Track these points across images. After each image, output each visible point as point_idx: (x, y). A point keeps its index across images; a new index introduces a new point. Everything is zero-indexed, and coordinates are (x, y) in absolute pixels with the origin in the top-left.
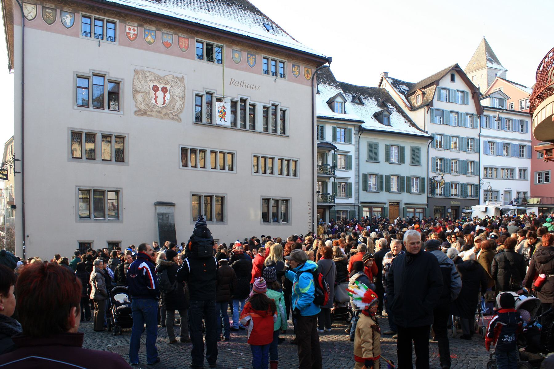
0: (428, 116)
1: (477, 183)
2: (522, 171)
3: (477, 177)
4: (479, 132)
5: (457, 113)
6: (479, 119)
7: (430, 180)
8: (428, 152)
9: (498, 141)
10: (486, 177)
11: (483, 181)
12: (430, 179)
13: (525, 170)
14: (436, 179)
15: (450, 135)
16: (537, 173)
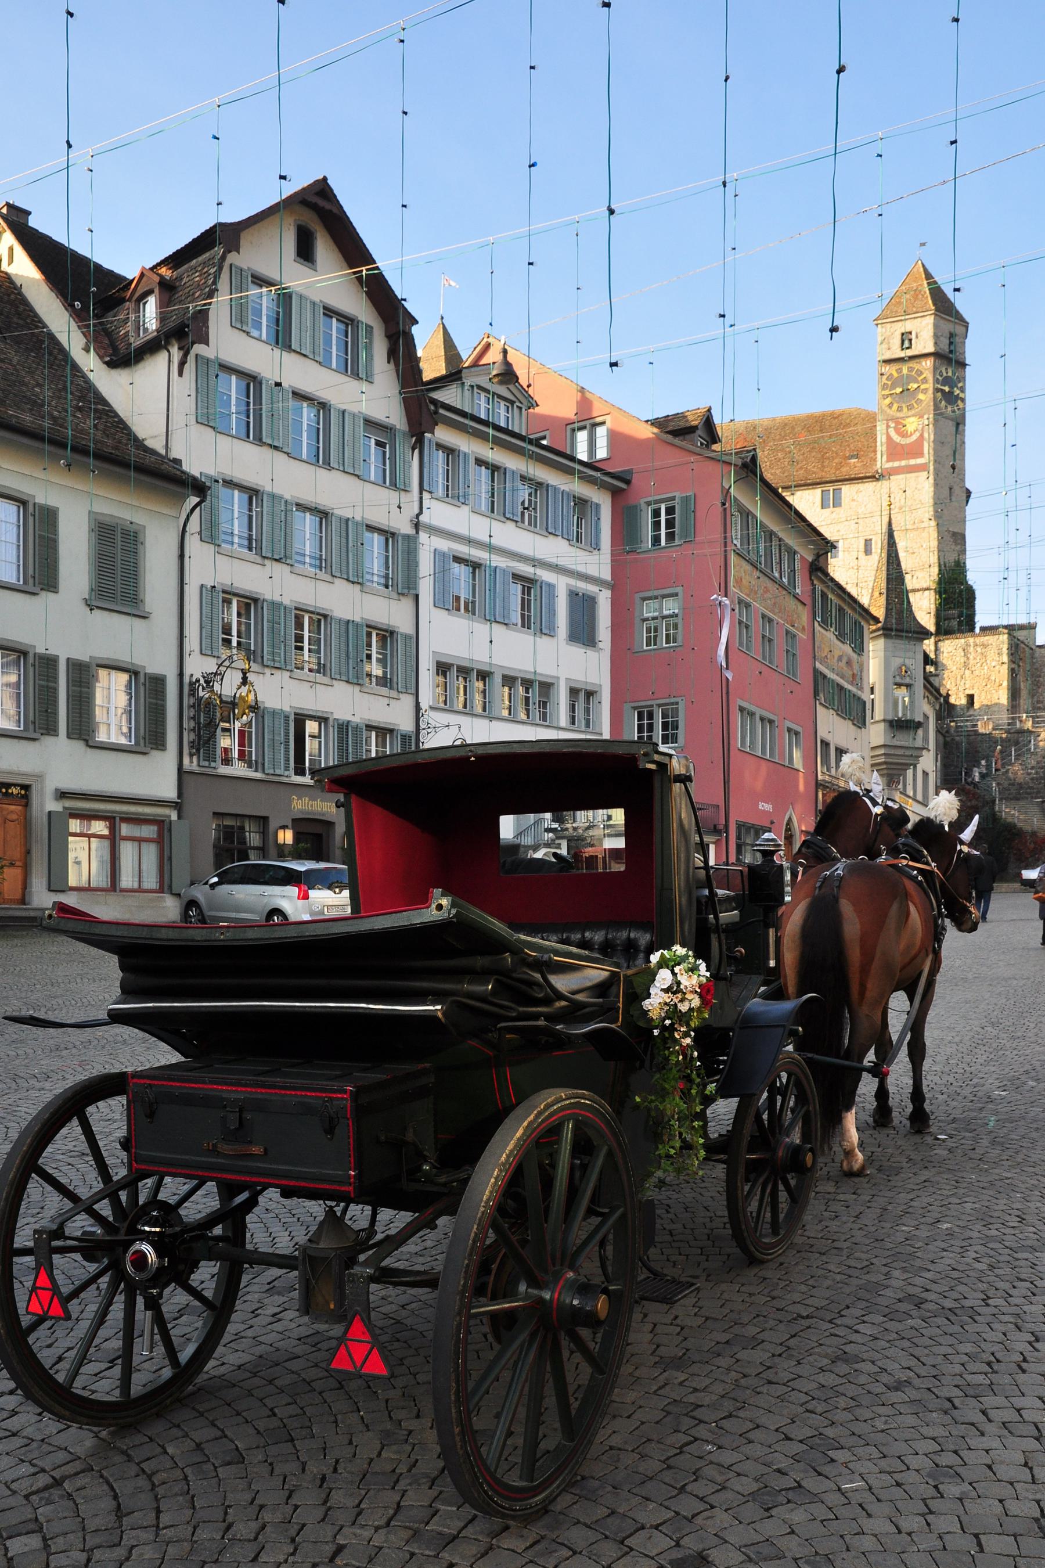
0: (185, 386)
1: (406, 725)
3: (407, 702)
4: (416, 511)
5: (323, 406)
6: (416, 451)
7: (193, 691)
8: (182, 556)
10: (446, 706)
12: (191, 684)
13: (589, 694)
14: (217, 687)
15: (287, 496)
16: (635, 708)
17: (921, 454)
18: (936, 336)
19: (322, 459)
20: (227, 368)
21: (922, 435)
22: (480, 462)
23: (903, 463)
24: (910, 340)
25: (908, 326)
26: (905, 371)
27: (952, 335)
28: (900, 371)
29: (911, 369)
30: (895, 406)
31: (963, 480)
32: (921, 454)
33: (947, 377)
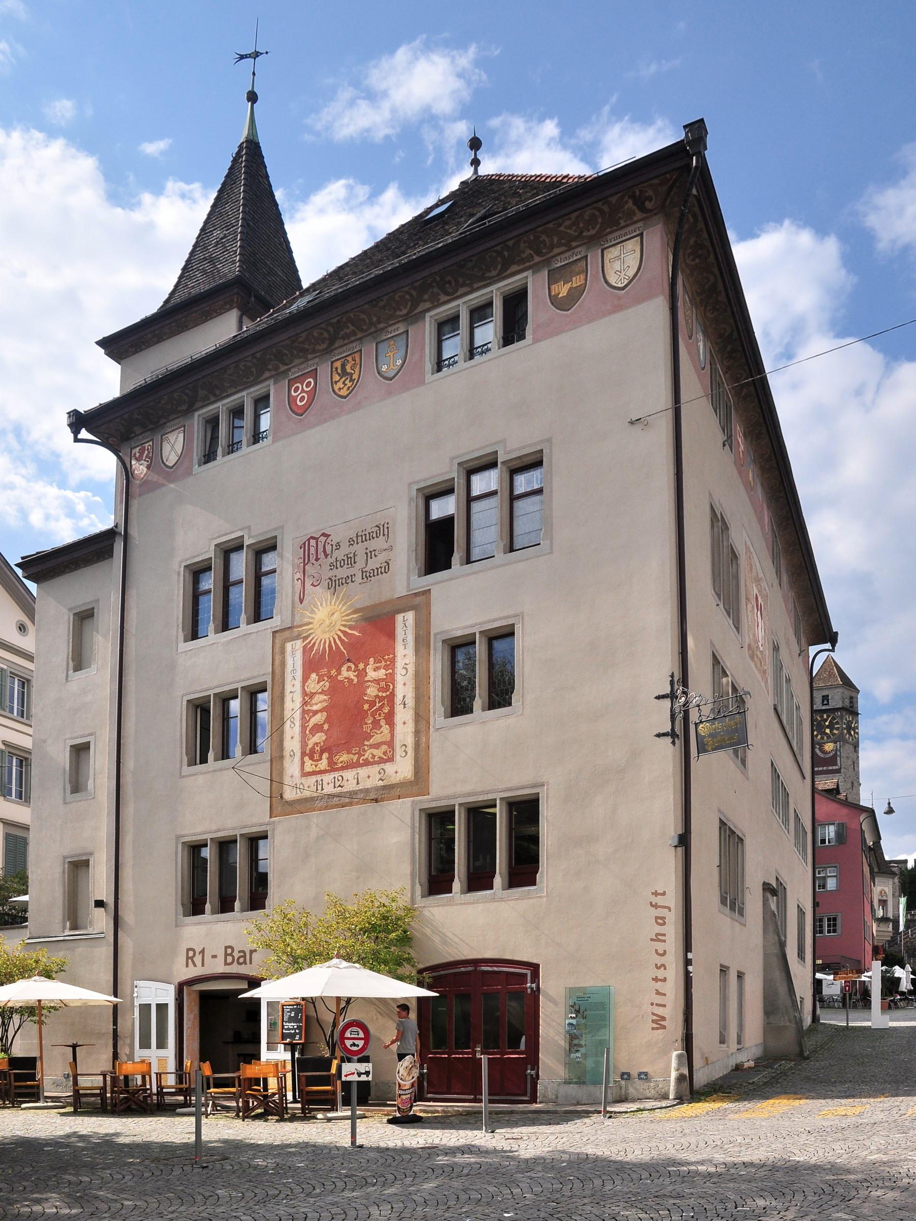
17: (836, 765)
18: (843, 699)
21: (836, 753)
23: (825, 768)
24: (828, 700)
26: (825, 716)
27: (851, 698)
28: (822, 717)
29: (828, 717)
31: (858, 778)
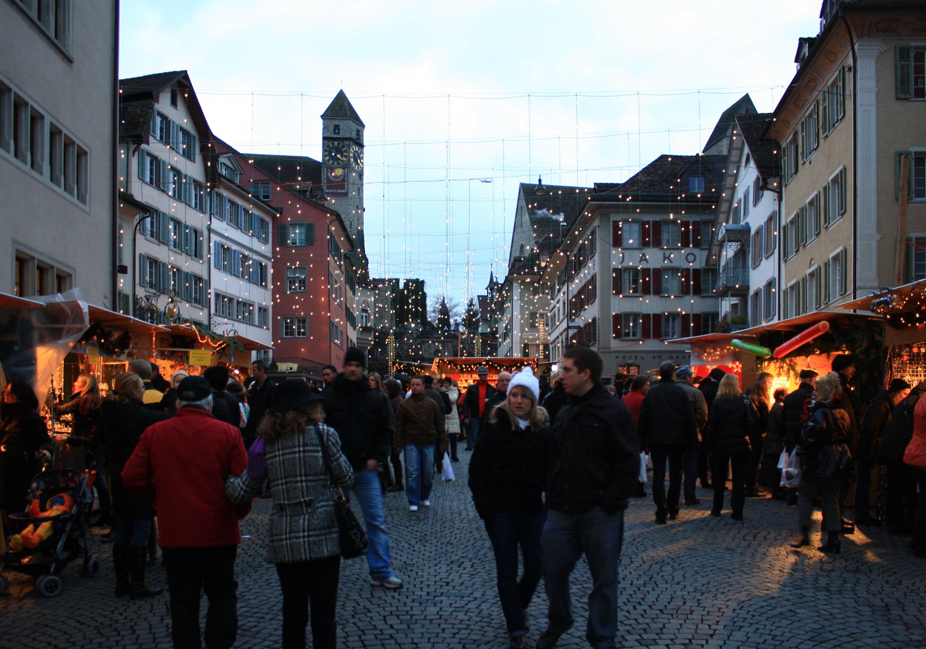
1: (206, 322)
2: (263, 310)
8: (134, 240)
9: (234, 247)
11: (216, 319)
17: (344, 189)
19: (179, 196)
20: (149, 154)
22: (229, 201)
25: (337, 123)
26: (336, 143)
27: (358, 131)
28: (333, 144)
30: (331, 162)
32: (344, 189)
33: (356, 151)
